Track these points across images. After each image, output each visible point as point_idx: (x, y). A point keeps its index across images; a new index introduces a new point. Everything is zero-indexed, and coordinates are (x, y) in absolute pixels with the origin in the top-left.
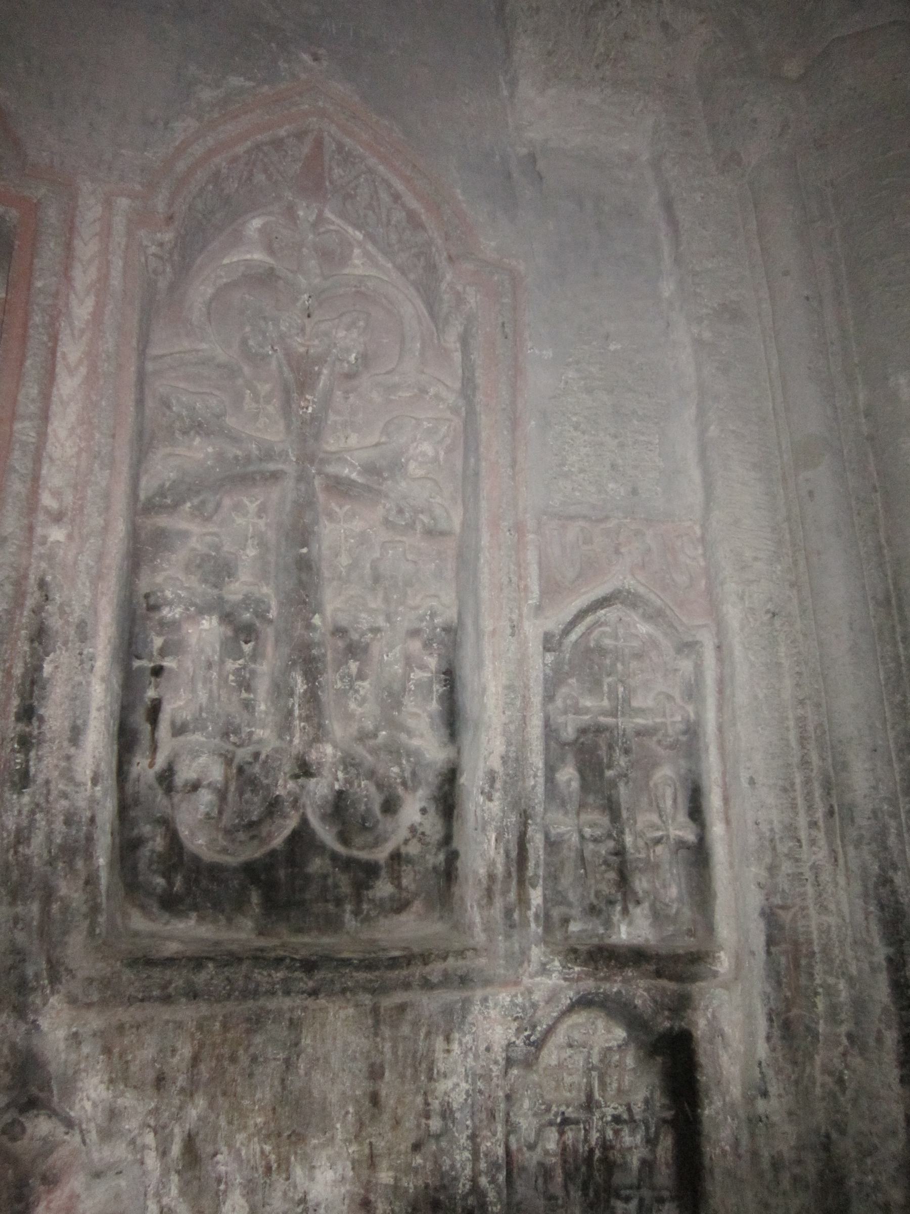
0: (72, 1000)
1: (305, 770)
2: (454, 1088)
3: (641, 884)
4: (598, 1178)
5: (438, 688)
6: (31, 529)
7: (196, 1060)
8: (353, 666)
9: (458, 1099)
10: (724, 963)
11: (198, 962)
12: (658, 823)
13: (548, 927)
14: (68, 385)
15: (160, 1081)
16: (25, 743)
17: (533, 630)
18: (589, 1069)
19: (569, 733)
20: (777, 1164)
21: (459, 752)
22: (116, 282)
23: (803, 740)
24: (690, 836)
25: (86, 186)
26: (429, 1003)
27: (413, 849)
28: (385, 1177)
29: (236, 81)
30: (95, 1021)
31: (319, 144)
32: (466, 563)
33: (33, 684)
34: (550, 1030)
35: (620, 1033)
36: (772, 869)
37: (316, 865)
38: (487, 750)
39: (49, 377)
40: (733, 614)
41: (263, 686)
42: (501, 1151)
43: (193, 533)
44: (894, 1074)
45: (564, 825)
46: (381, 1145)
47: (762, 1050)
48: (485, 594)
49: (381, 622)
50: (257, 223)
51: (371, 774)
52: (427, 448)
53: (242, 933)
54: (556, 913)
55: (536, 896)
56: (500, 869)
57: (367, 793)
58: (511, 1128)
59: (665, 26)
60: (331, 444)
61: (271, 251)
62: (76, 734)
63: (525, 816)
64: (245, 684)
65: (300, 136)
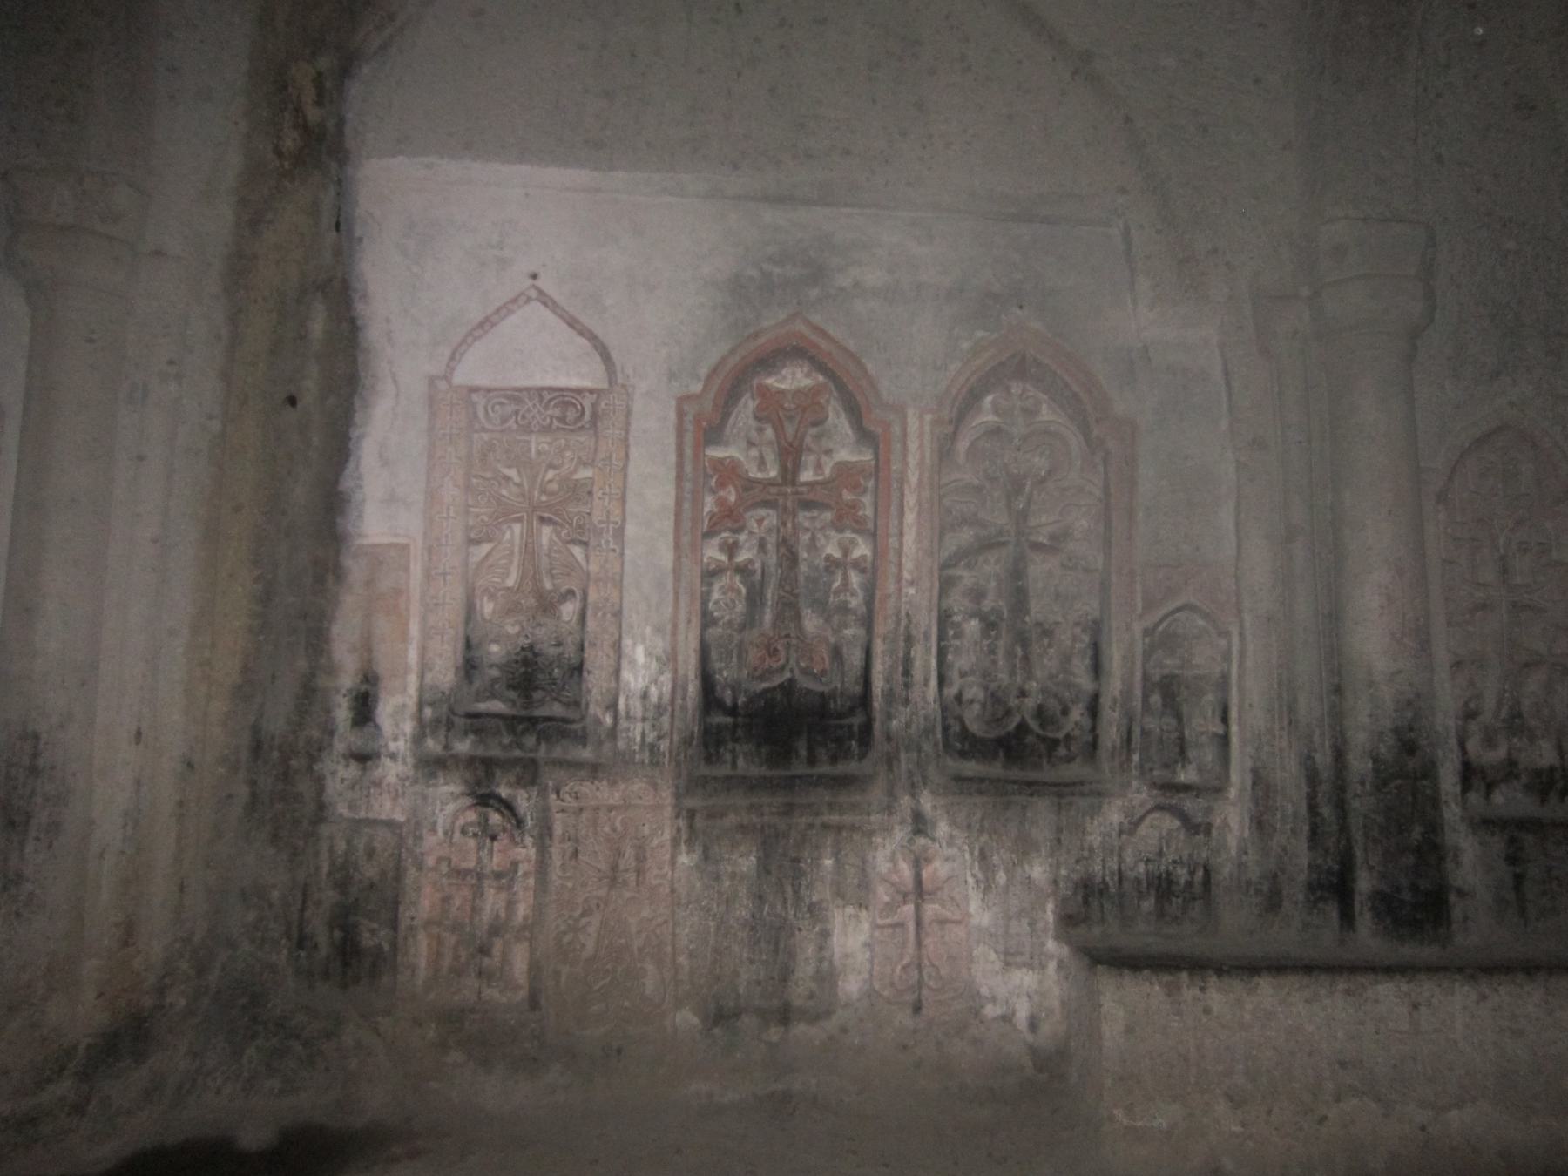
0: (932, 792)
1: (1023, 694)
2: (1095, 839)
3: (1192, 753)
4: (1164, 885)
5: (1090, 653)
6: (900, 590)
7: (982, 819)
8: (1046, 641)
9: (1096, 844)
10: (1233, 793)
11: (982, 780)
12: (1202, 724)
13: (1142, 773)
14: (910, 518)
15: (969, 826)
16: (907, 686)
17: (1137, 628)
18: (1161, 838)
19: (1157, 678)
20: (1248, 883)
22: (928, 461)
23: (1279, 684)
25: (910, 412)
26: (1082, 803)
27: (1077, 733)
28: (1063, 872)
29: (980, 334)
32: (1105, 587)
33: (907, 662)
34: (1142, 819)
35: (1177, 823)
36: (1258, 749)
37: (1030, 739)
38: (1114, 686)
40: (1247, 618)
41: (1001, 652)
42: (1116, 867)
43: (967, 577)
45: (1152, 724)
46: (1062, 859)
47: (1247, 833)
49: (1060, 619)
50: (989, 399)
51: (1056, 696)
52: (1084, 523)
53: (996, 769)
54: (1147, 766)
55: (1136, 758)
57: (1053, 706)
58: (1121, 861)
59: (1227, 264)
60: (1033, 522)
62: (926, 682)
63: (1131, 720)
64: (992, 651)
65: (1014, 356)
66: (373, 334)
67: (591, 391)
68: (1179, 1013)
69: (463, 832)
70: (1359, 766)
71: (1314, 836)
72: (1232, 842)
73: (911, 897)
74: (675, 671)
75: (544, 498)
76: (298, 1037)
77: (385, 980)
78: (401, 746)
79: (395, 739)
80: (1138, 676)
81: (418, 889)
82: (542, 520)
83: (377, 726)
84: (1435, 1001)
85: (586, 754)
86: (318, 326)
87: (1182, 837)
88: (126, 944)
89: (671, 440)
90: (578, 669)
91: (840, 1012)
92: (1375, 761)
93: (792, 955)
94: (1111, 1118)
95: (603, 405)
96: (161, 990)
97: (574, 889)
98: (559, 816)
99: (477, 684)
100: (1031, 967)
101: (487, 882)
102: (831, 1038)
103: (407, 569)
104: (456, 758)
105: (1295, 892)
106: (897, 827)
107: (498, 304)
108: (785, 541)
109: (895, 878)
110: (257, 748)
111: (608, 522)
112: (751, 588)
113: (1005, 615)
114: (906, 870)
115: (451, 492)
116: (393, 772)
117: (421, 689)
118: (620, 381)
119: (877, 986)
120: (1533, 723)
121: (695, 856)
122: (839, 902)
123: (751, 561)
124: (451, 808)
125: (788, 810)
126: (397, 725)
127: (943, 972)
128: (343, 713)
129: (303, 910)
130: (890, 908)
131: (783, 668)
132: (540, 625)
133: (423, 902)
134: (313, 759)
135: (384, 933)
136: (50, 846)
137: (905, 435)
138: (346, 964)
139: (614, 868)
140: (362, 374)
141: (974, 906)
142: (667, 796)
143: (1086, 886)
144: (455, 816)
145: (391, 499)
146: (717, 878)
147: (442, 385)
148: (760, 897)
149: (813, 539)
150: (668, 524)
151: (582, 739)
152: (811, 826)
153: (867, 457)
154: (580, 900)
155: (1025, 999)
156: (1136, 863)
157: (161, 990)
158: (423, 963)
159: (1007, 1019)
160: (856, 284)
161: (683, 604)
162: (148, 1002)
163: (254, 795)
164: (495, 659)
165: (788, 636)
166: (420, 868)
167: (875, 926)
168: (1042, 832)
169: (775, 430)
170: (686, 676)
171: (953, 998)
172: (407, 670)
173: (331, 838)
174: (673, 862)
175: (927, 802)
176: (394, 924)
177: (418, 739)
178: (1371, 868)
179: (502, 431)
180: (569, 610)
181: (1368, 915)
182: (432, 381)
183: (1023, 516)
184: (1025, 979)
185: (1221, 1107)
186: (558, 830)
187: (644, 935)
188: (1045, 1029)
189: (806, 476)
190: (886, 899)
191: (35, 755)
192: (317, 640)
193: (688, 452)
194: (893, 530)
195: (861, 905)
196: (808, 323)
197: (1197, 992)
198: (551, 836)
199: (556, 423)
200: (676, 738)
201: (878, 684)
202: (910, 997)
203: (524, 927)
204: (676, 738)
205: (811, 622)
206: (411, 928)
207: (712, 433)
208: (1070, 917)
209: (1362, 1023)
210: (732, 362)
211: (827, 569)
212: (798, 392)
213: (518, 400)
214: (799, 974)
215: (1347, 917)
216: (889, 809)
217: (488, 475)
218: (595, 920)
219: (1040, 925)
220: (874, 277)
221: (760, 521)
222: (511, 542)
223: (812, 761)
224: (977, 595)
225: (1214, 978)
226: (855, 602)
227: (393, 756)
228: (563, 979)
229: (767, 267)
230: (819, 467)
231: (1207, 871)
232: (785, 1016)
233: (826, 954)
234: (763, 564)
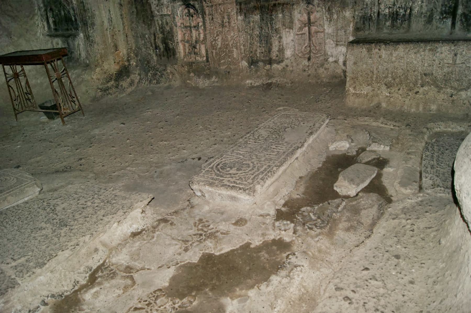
4: (395, 16)
20: (422, 13)
58: (380, 8)
76: (158, 71)
81: (177, 32)
84: (464, 53)
91: (286, 60)
93: (271, 45)
94: (349, 90)
96: (128, 61)
101: (192, 29)
105: (437, 16)
109: (302, 19)
114: (305, 16)
124: (180, 9)
129: (155, 40)
130: (301, 29)
133: (179, 36)
138: (168, 53)
143: (364, 18)
146: (249, 23)
152: (275, 5)
154: (215, 32)
155: (342, 55)
156: (385, 8)
157: (128, 61)
162: (126, 64)
163: (137, 10)
166: (176, 26)
173: (157, 20)
174: (237, 19)
178: (463, 5)
181: (459, 23)
185: (384, 87)
186: (207, 13)
187: (232, 41)
190: (300, 26)
191: (84, 7)
197: (377, 50)
198: (205, 14)
202: (307, 56)
203: (202, 41)
208: (358, 28)
209: (434, 60)
214: (273, 50)
219: (348, 32)
225: (384, 46)
228: (214, 54)
232: (270, 62)
233: (281, 44)
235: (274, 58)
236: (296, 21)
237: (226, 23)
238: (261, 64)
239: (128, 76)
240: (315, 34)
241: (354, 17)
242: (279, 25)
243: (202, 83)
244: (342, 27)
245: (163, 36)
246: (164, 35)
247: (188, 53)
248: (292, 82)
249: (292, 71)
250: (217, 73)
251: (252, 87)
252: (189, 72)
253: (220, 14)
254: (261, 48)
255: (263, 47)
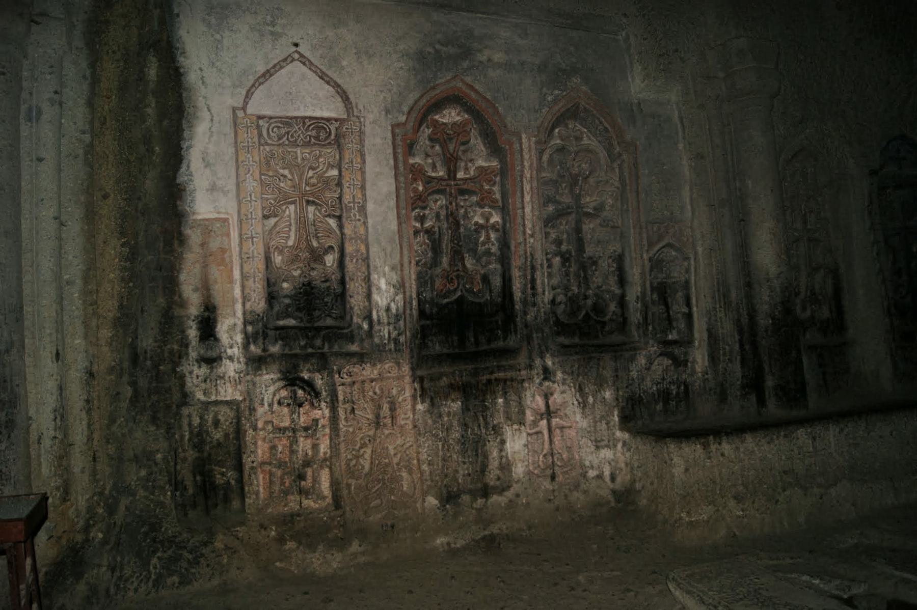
0: (553, 356)
2: (634, 374)
3: (674, 324)
6: (525, 239)
9: (635, 376)
12: (678, 308)
14: (527, 198)
16: (534, 295)
19: (655, 284)
21: (624, 291)
22: (535, 165)
23: (718, 283)
24: (685, 310)
25: (524, 136)
26: (627, 355)
27: (614, 317)
29: (556, 92)
30: (557, 360)
31: (578, 107)
33: (533, 281)
35: (670, 362)
36: (710, 319)
39: (523, 197)
40: (700, 250)
44: (739, 366)
47: (707, 364)
48: (633, 247)
50: (557, 130)
52: (610, 201)
55: (650, 328)
56: (641, 321)
59: (681, 58)
61: (562, 140)
63: (647, 307)
64: (567, 275)
66: (192, 78)
67: (336, 120)
68: (710, 458)
69: (279, 403)
70: (763, 322)
71: (743, 362)
72: (698, 369)
73: (545, 416)
74: (404, 293)
75: (308, 188)
76: (185, 548)
77: (236, 504)
78: (236, 351)
79: (231, 347)
80: (648, 283)
81: (255, 444)
82: (308, 202)
83: (217, 340)
85: (354, 348)
86: (152, 72)
87: (673, 368)
88: (64, 500)
89: (390, 150)
90: (342, 296)
92: (773, 319)
93: (486, 457)
95: (344, 129)
97: (353, 432)
98: (340, 388)
99: (276, 308)
100: (608, 446)
102: (511, 501)
103: (228, 235)
104: (271, 355)
106: (536, 377)
107: (276, 61)
108: (452, 214)
109: (534, 405)
110: (135, 359)
111: (354, 202)
112: (433, 241)
113: (573, 254)
114: (540, 401)
115: (251, 185)
116: (232, 369)
117: (244, 314)
118: (355, 114)
119: (531, 468)
120: (820, 297)
121: (426, 405)
122: (509, 423)
123: (433, 227)
124: (272, 389)
125: (475, 373)
126: (231, 338)
127: (564, 456)
128: (193, 333)
129: (176, 464)
130: (535, 423)
131: (455, 290)
132: (313, 269)
133: (259, 449)
134: (176, 364)
135: (231, 474)
136: (9, 437)
137: (522, 149)
138: (206, 498)
139: (378, 417)
140: (187, 105)
141: (578, 417)
142: (406, 369)
143: (632, 399)
144: (274, 395)
145: (213, 188)
146: (440, 416)
147: (240, 114)
148: (466, 425)
149: (466, 212)
150: (393, 203)
151: (351, 338)
152: (489, 381)
153: (495, 163)
154: (358, 439)
157: (87, 529)
158: (261, 490)
159: (600, 477)
160: (489, 60)
161: (405, 252)
164: (286, 292)
165: (458, 270)
166: (255, 429)
167: (529, 434)
168: (608, 373)
169: (440, 146)
170: (411, 297)
171: (571, 470)
172: (234, 301)
173: (189, 416)
175: (549, 363)
176: (239, 467)
177: (246, 346)
179: (279, 145)
180: (330, 260)
182: (234, 110)
183: (578, 198)
184: (606, 453)
185: (732, 503)
186: (341, 398)
187: (399, 456)
188: (619, 480)
189: (460, 175)
190: (532, 418)
192: (171, 285)
193: (400, 157)
194: (519, 205)
195: (522, 423)
196: (462, 80)
198: (337, 400)
199: (313, 140)
200: (408, 333)
201: (518, 295)
203: (325, 460)
204: (408, 333)
205: (469, 263)
206: (252, 468)
207: (410, 148)
210: (421, 103)
211: (476, 230)
212: (455, 123)
213: (288, 124)
214: (490, 467)
215: (761, 402)
216: (530, 367)
217: (271, 173)
218: (368, 451)
219: (612, 423)
220: (498, 57)
221: (436, 201)
222: (289, 216)
223: (477, 343)
224: (558, 242)
226: (494, 249)
227: (231, 358)
229: (438, 46)
230: (467, 169)
231: (686, 387)
232: (485, 492)
233: (504, 454)
234: (439, 228)
235: (492, 483)
236: (528, 413)
237: (385, 418)
238: (466, 498)
239: (79, 576)
240: (558, 431)
241: (617, 399)
242: (499, 418)
243: (323, 562)
244: (602, 417)
245: (197, 455)
246: (199, 451)
247: (281, 491)
248: (530, 528)
249: (528, 503)
250: (363, 533)
251: (453, 553)
252: (281, 540)
253: (372, 400)
254: (466, 466)
255: (471, 463)
